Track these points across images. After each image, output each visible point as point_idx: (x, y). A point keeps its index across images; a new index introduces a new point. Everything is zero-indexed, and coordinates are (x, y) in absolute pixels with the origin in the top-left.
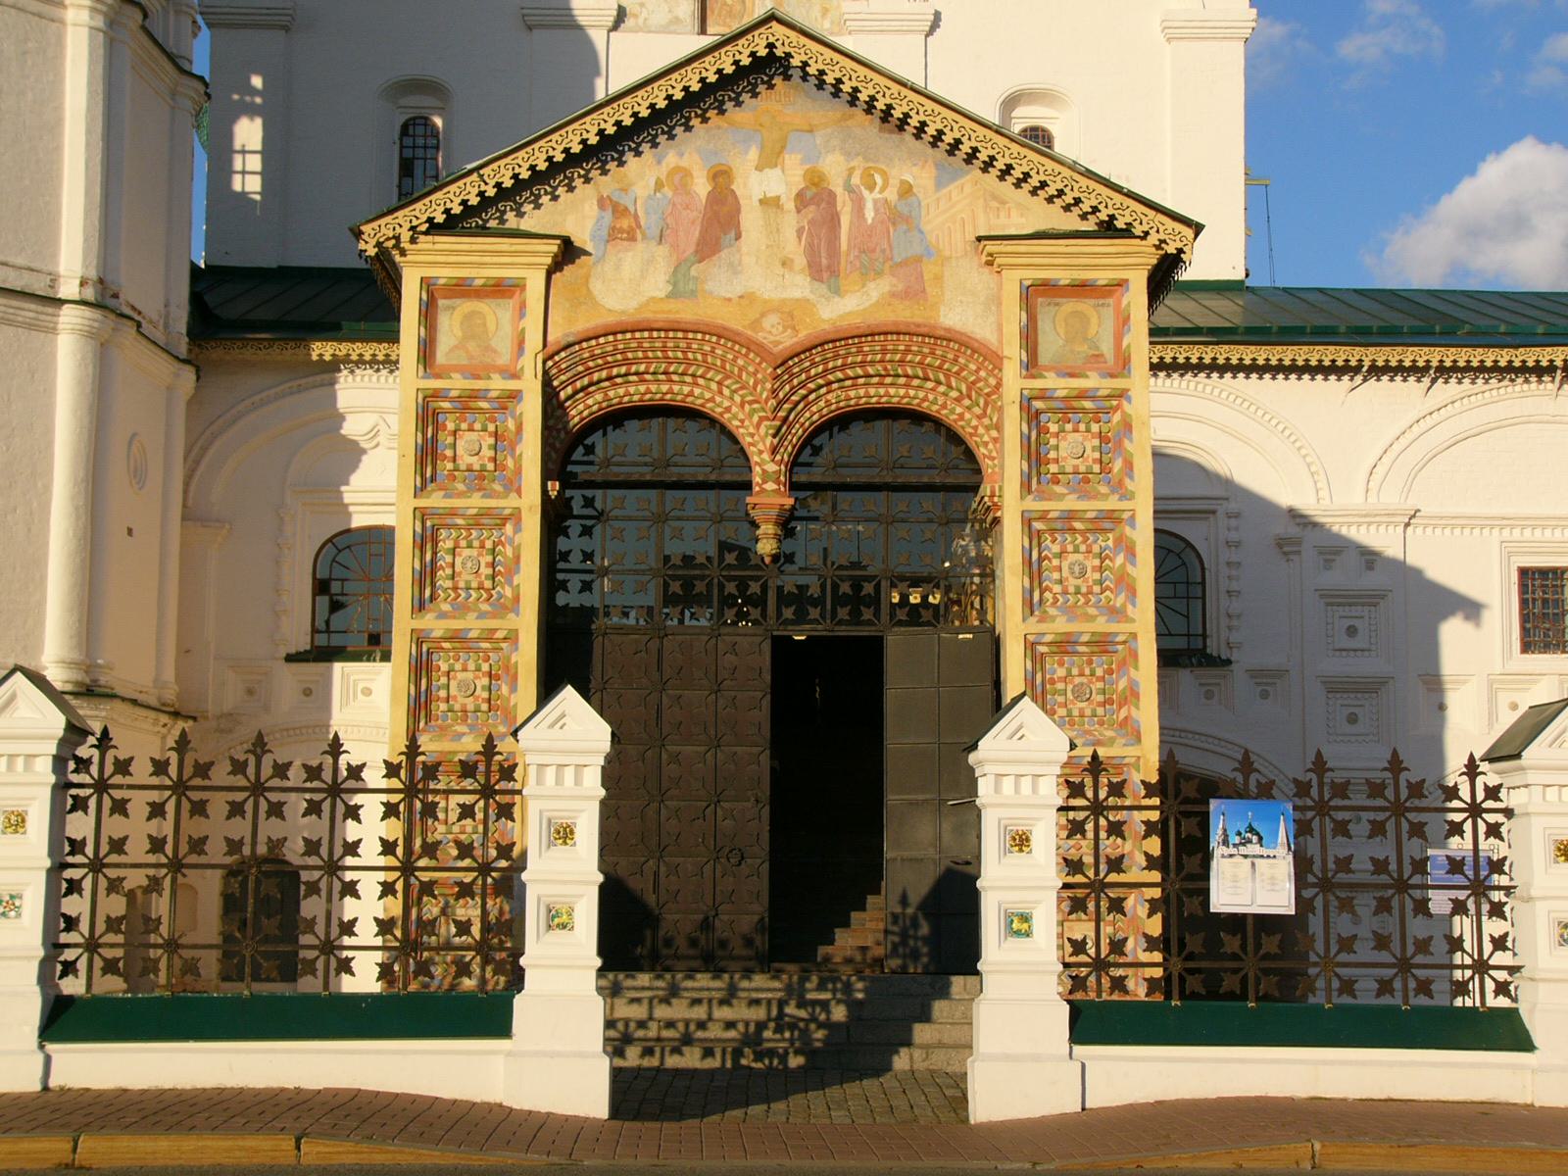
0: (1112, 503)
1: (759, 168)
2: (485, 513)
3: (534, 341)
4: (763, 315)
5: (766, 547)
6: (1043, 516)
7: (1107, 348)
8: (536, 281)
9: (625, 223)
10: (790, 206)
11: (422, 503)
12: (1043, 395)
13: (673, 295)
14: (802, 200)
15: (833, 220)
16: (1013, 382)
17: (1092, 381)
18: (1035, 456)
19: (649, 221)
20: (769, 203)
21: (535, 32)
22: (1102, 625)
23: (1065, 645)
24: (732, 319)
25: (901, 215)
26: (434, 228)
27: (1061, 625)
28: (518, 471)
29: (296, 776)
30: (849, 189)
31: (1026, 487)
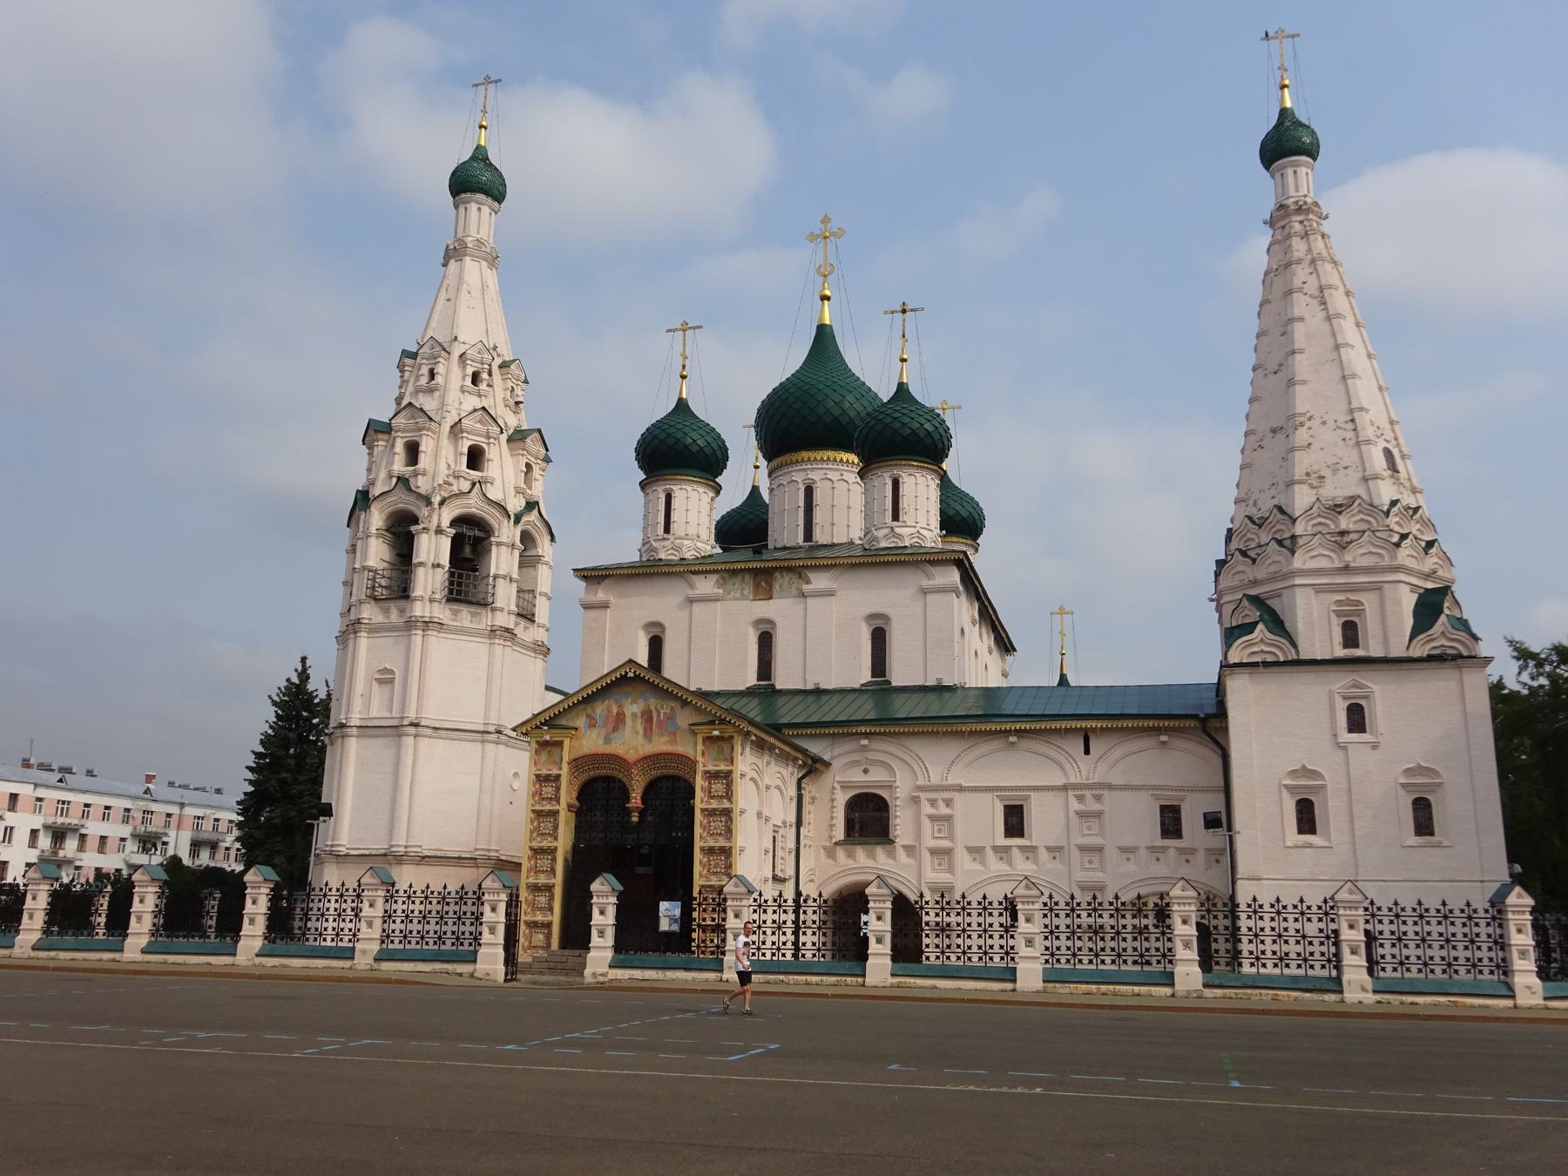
0: (726, 804)
1: (631, 704)
2: (550, 811)
3: (566, 759)
4: (630, 749)
6: (706, 810)
7: (728, 757)
9: (593, 722)
10: (639, 715)
11: (533, 808)
12: (707, 772)
13: (605, 744)
14: (643, 713)
15: (652, 718)
16: (700, 768)
17: (723, 767)
20: (634, 715)
21: (696, 607)
22: (722, 843)
23: (709, 851)
25: (671, 717)
26: (537, 727)
27: (711, 843)
29: (436, 894)
30: (656, 708)
31: (702, 801)
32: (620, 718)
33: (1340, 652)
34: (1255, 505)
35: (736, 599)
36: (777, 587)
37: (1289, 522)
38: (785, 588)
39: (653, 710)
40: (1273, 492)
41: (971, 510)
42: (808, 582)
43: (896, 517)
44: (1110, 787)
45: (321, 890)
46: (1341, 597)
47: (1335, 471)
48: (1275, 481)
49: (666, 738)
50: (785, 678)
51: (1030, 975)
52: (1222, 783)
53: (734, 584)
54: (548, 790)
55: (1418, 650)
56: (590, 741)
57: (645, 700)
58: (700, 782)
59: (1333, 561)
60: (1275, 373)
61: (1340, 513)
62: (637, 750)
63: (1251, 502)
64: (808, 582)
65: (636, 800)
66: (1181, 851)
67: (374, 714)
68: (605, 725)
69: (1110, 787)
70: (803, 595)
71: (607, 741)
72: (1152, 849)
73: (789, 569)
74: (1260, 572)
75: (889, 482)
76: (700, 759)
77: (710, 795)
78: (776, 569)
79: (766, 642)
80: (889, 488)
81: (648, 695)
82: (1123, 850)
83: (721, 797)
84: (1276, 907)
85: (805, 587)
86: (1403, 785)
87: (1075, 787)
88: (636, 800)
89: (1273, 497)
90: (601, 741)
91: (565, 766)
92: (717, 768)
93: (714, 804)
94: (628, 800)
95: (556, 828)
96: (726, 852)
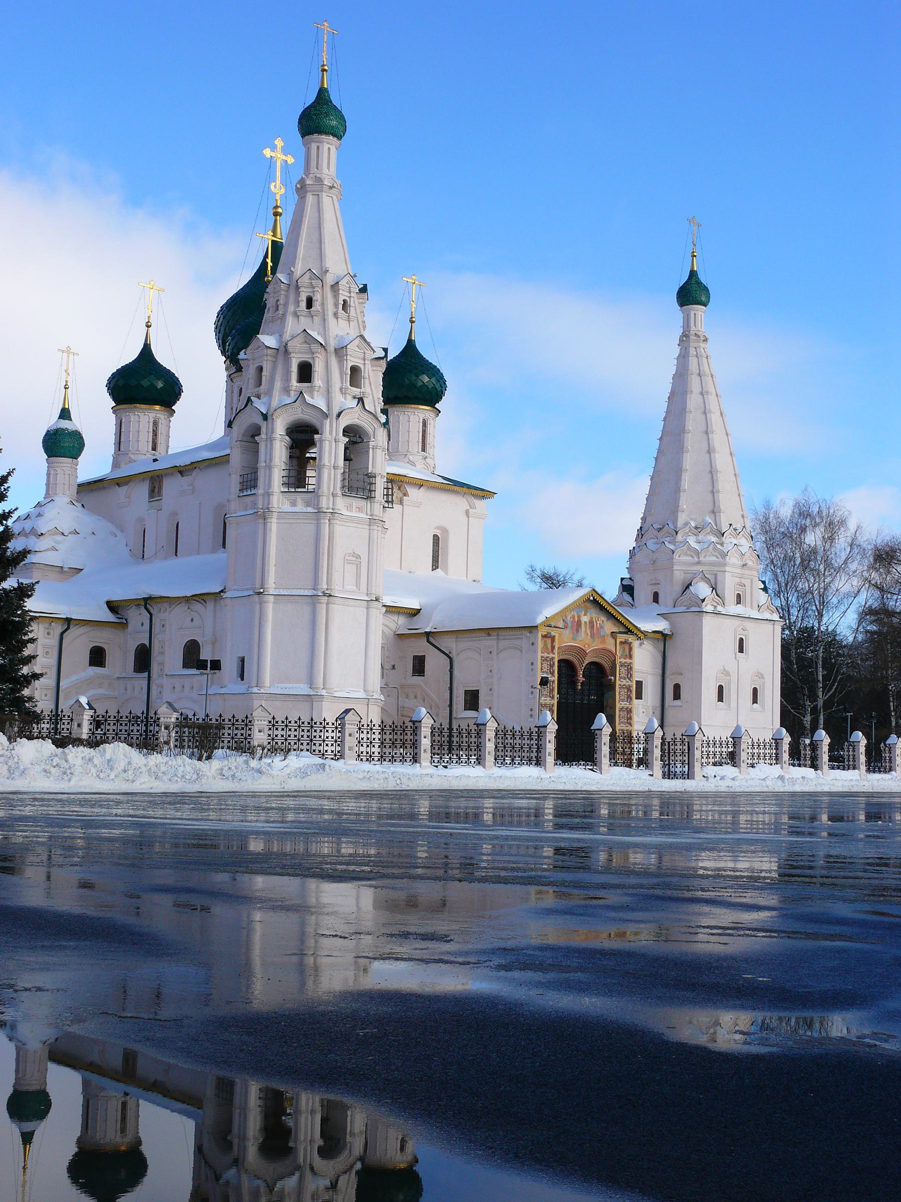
12: (620, 662)
14: (590, 622)
15: (592, 627)
17: (628, 661)
19: (570, 624)
20: (585, 622)
32: (579, 624)
39: (594, 620)
42: (405, 494)
43: (423, 450)
45: (321, 723)
59: (718, 558)
67: (348, 587)
81: (592, 610)
84: (298, 723)
92: (625, 661)
95: (552, 690)
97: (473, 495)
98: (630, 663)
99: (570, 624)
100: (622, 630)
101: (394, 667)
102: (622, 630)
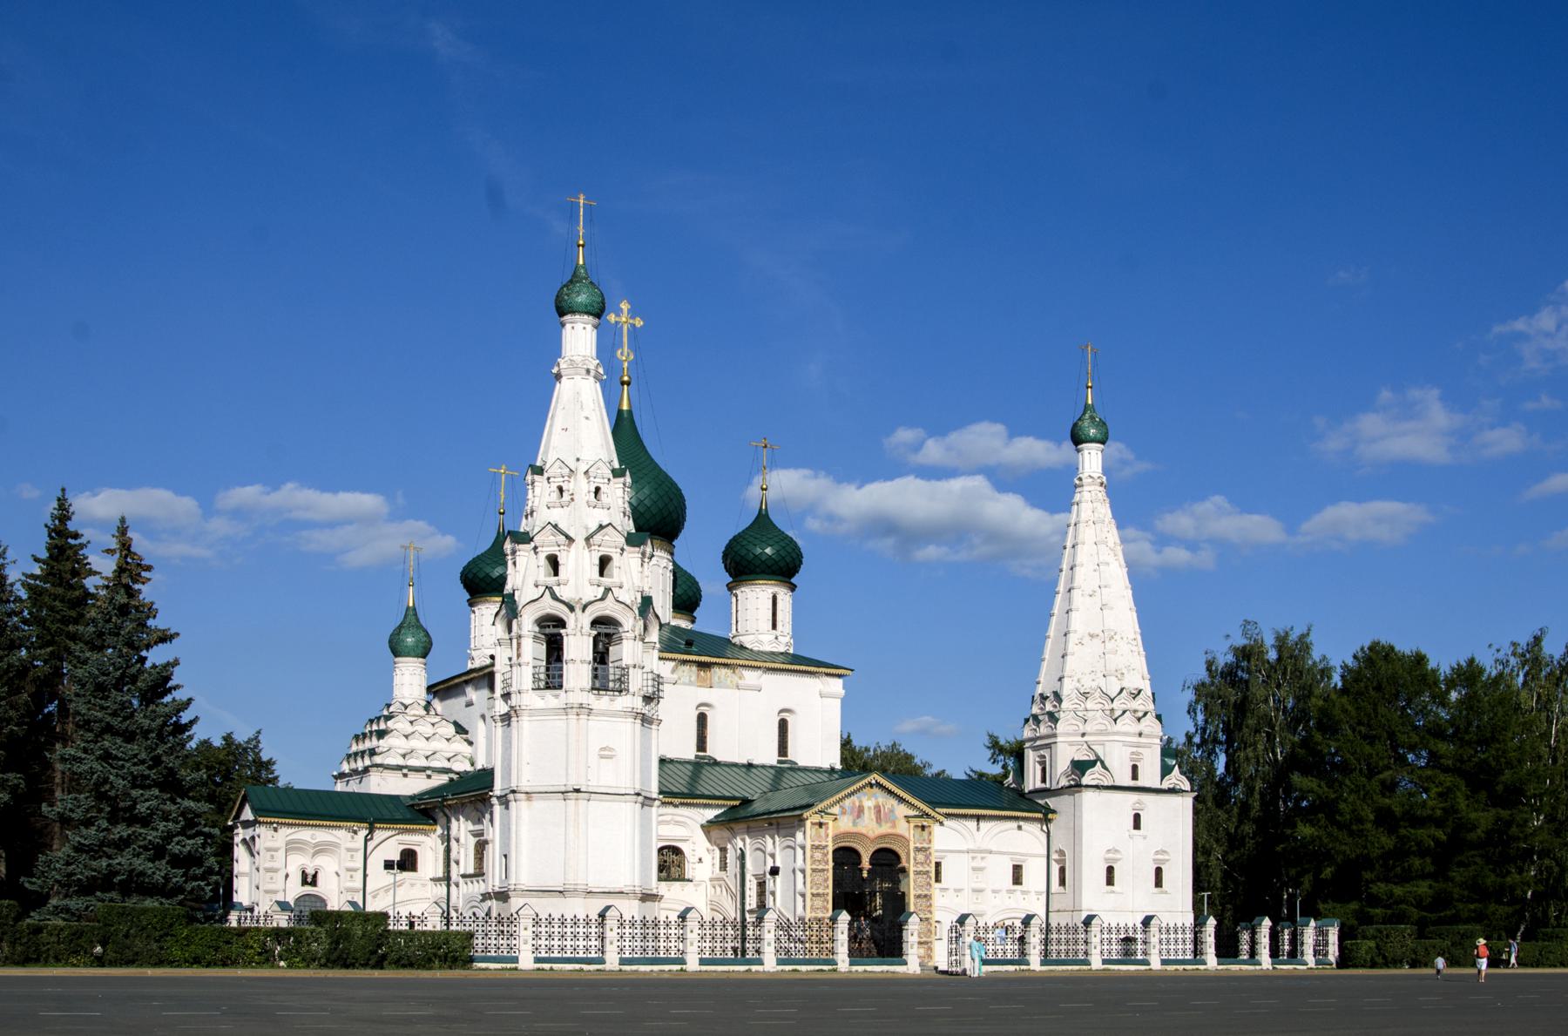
5: (865, 875)
7: (926, 838)
8: (831, 823)
12: (916, 848)
14: (875, 807)
15: (879, 811)
17: (925, 845)
18: (915, 859)
19: (848, 811)
20: (869, 808)
22: (926, 892)
23: (919, 896)
24: (864, 831)
25: (892, 811)
27: (919, 892)
28: (828, 861)
32: (861, 810)
33: (1132, 783)
34: (1078, 681)
35: (684, 684)
36: (716, 679)
37: (1110, 702)
38: (722, 679)
39: (880, 804)
40: (1093, 675)
41: (695, 590)
42: (741, 678)
43: (774, 626)
44: (991, 852)
46: (1134, 749)
47: (1129, 671)
48: (1094, 670)
49: (889, 825)
50: (717, 750)
51: (1155, 964)
52: (1046, 853)
53: (684, 672)
54: (818, 855)
55: (1166, 785)
56: (845, 824)
57: (876, 799)
58: (912, 854)
60: (1091, 596)
61: (1134, 698)
62: (874, 832)
63: (1075, 679)
64: (741, 678)
65: (866, 863)
66: (1023, 892)
68: (851, 813)
69: (991, 852)
70: (738, 687)
71: (855, 824)
72: (1009, 891)
73: (726, 665)
74: (1088, 728)
75: (771, 596)
76: (912, 838)
77: (916, 863)
78: (716, 663)
79: (702, 720)
80: (771, 601)
82: (994, 891)
83: (922, 863)
85: (740, 682)
86: (1154, 860)
87: (973, 851)
88: (866, 863)
89: (1093, 680)
90: (851, 824)
91: (830, 839)
92: (922, 846)
93: (920, 868)
94: (860, 863)
95: (826, 880)
96: (927, 897)
97: (828, 675)
98: (929, 848)
99: (848, 811)
100: (915, 813)
101: (700, 859)
102: (915, 813)
